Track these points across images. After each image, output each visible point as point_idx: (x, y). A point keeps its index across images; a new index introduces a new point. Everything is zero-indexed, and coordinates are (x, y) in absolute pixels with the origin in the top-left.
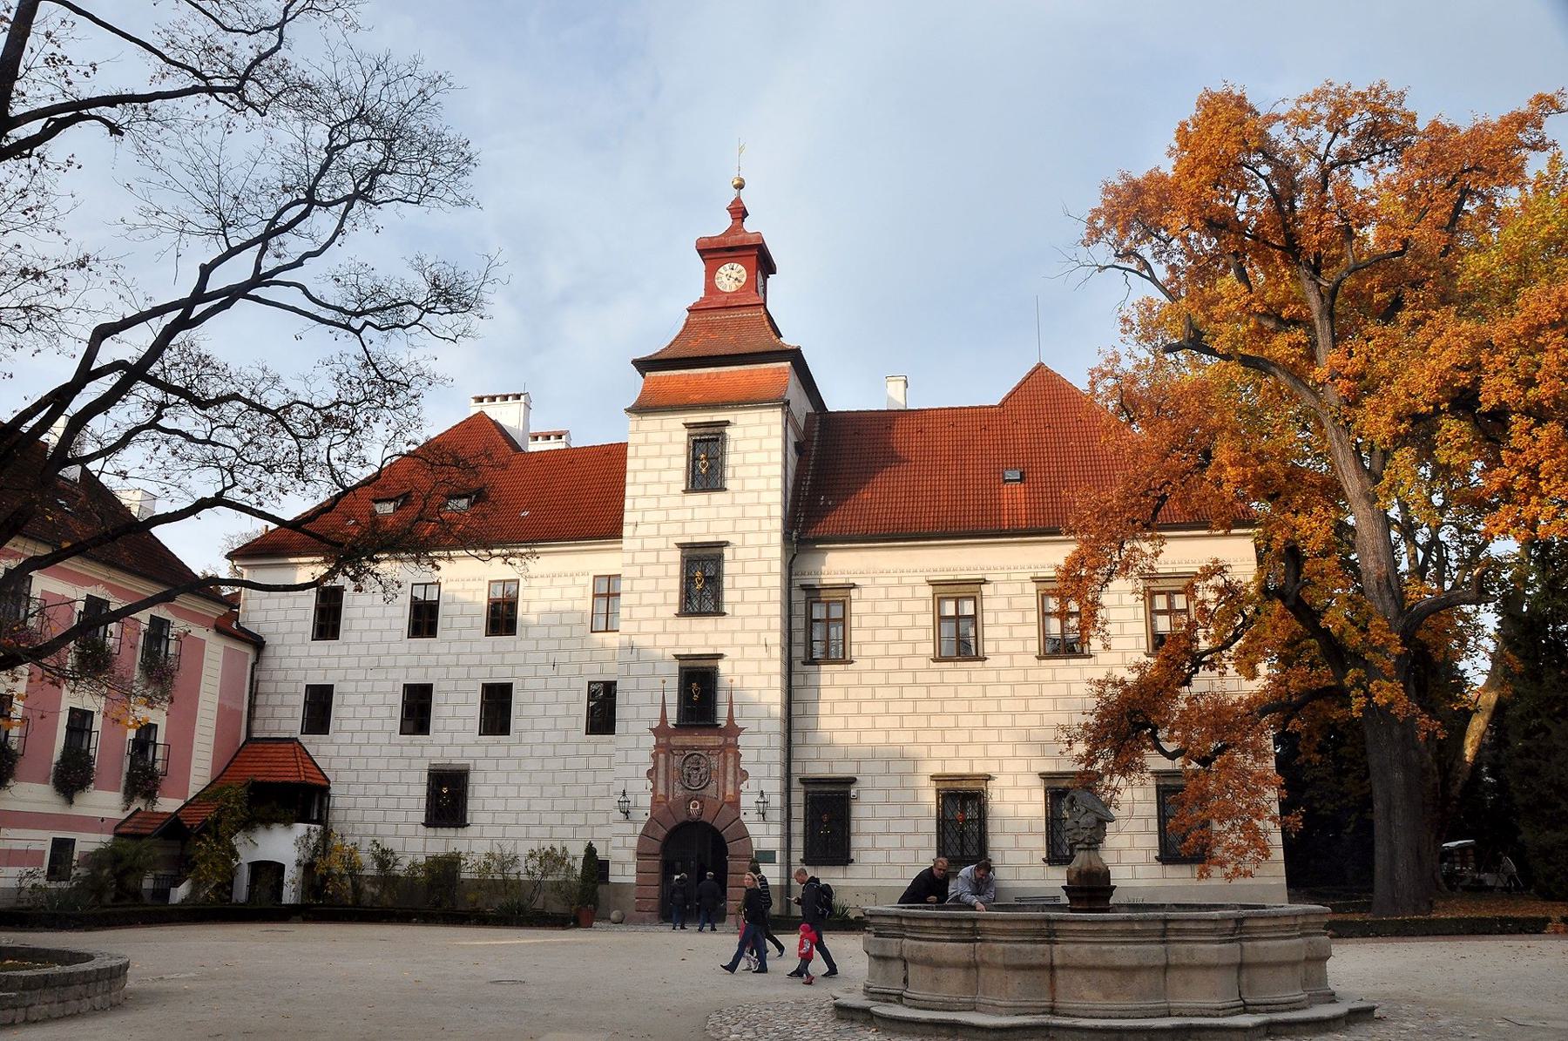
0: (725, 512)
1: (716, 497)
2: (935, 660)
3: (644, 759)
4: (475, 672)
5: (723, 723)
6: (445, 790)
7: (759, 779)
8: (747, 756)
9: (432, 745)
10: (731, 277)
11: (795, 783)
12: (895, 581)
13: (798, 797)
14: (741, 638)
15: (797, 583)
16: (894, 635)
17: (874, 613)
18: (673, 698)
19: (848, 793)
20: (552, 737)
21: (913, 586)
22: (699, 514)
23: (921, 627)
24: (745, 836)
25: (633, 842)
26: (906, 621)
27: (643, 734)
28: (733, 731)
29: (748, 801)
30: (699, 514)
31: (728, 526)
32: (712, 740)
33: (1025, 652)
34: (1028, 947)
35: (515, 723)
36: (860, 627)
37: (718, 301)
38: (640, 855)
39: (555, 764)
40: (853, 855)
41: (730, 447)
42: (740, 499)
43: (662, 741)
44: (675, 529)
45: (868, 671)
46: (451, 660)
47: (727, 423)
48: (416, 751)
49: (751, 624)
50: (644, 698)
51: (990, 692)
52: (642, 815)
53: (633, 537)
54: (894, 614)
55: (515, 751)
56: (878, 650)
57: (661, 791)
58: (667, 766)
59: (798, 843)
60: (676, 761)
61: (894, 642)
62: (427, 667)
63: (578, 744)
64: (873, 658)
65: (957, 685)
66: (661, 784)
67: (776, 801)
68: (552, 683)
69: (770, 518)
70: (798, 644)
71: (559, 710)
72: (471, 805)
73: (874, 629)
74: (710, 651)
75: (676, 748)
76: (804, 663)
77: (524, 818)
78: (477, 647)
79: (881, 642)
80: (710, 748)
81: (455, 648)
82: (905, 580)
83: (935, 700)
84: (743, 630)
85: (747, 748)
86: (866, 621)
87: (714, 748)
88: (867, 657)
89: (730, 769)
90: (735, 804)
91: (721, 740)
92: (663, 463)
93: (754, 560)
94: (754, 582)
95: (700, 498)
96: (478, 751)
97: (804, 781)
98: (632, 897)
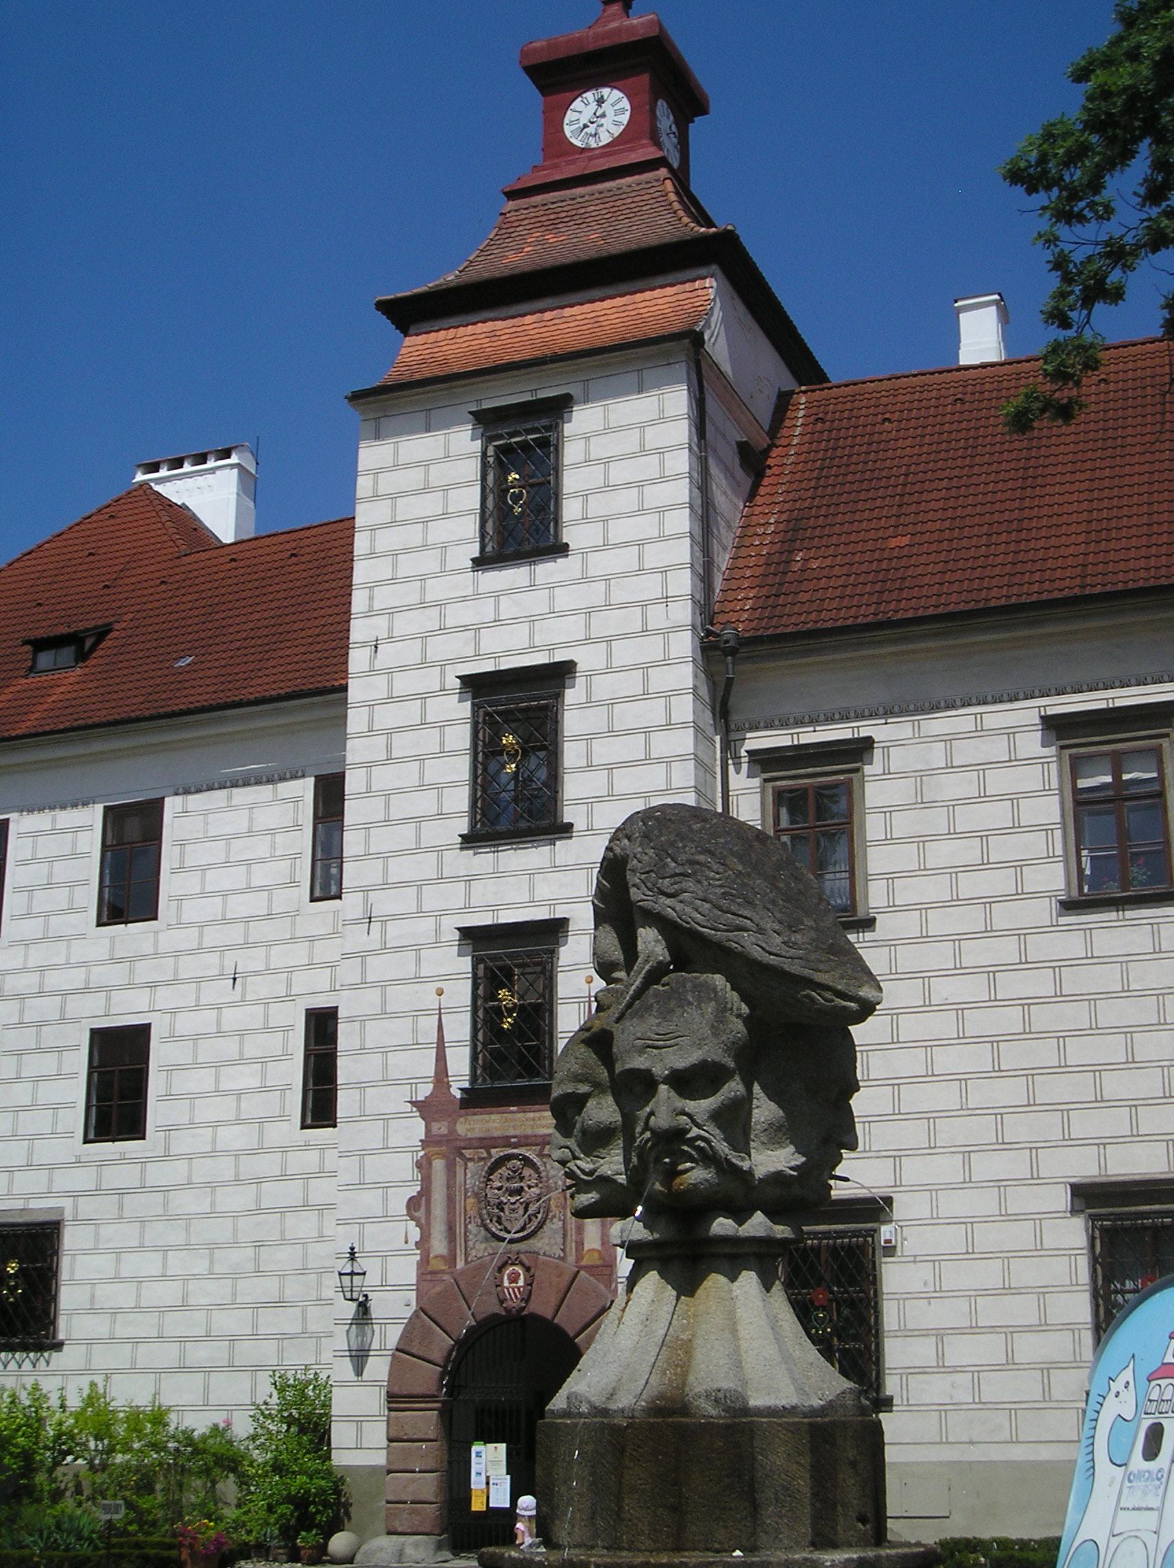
0: (566, 599)
1: (547, 570)
3: (400, 1170)
4: (76, 1006)
16: (969, 852)
17: (923, 803)
18: (460, 1028)
20: (232, 1137)
22: (508, 608)
23: (1033, 829)
26: (998, 814)
27: (398, 1116)
30: (508, 608)
31: (572, 628)
35: (156, 1113)
36: (889, 840)
38: (396, 1400)
39: (240, 1199)
41: (571, 452)
42: (601, 563)
43: (441, 1128)
44: (458, 645)
50: (399, 1030)
52: (395, 1307)
53: (372, 671)
54: (967, 801)
55: (159, 1174)
56: (934, 889)
57: (439, 1246)
58: (450, 1186)
60: (470, 1175)
61: (969, 868)
63: (284, 1150)
64: (923, 908)
65: (1126, 960)
68: (232, 1018)
69: (666, 599)
71: (246, 1078)
72: (69, 1297)
73: (922, 841)
74: (541, 914)
75: (471, 1143)
77: (176, 1324)
78: (80, 951)
79: (938, 871)
81: (37, 956)
83: (1074, 998)
86: (903, 824)
88: (907, 908)
92: (430, 505)
93: (633, 699)
95: (513, 576)
96: (82, 1179)
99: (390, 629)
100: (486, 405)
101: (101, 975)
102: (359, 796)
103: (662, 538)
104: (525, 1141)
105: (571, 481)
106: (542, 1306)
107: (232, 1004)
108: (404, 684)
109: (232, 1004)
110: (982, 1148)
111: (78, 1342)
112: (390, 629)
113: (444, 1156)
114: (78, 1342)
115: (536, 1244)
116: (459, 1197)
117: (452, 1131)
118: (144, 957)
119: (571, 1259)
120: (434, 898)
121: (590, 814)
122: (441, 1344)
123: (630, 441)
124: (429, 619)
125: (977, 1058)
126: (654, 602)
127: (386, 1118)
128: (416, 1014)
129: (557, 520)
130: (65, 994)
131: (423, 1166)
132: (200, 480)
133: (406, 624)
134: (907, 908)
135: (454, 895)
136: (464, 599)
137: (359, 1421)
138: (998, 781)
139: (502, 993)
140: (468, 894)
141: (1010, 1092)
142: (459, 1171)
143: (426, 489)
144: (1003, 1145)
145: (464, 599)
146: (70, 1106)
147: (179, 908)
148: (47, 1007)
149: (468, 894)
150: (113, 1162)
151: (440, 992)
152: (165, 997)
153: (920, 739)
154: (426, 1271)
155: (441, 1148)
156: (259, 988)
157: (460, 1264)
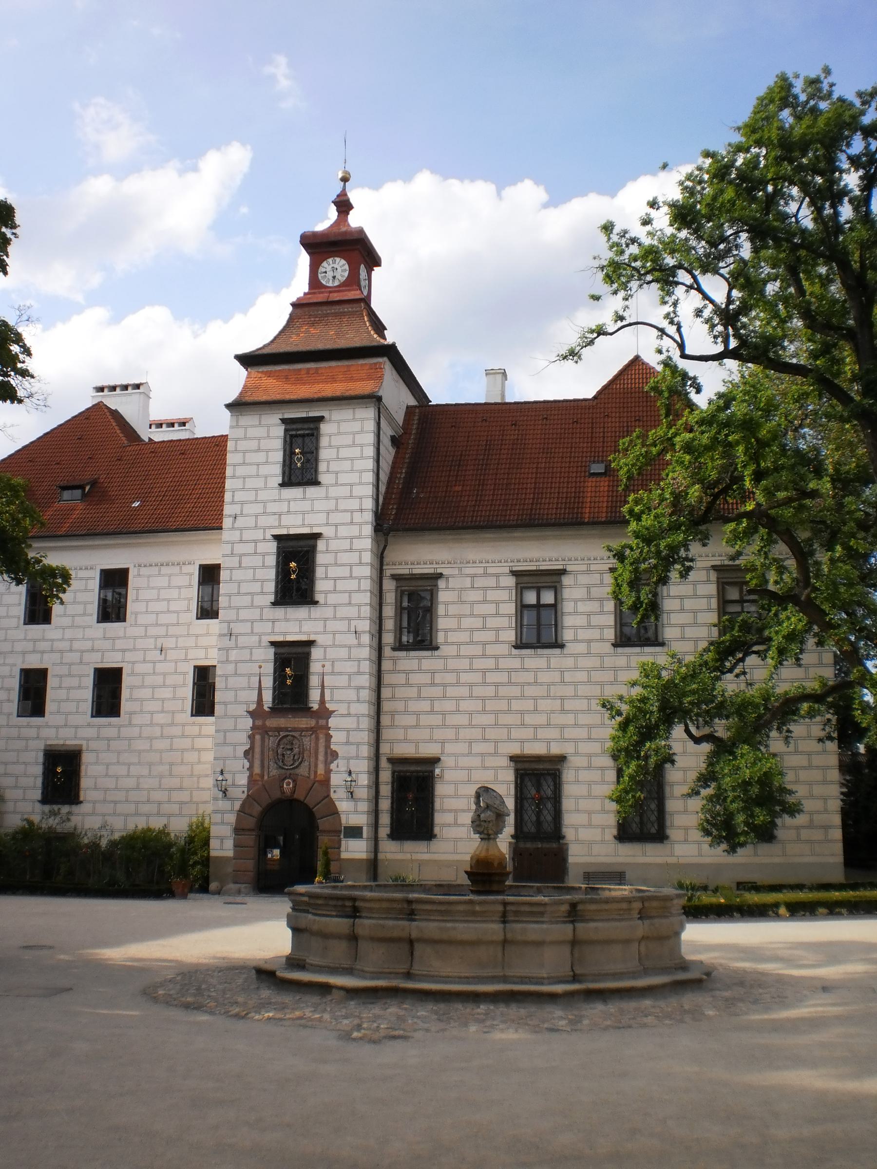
0: (319, 505)
1: (312, 491)
2: (516, 647)
3: (241, 739)
4: (87, 657)
5: (315, 706)
6: (59, 770)
7: (348, 759)
8: (337, 737)
9: (48, 726)
10: (336, 269)
11: (384, 763)
12: (481, 571)
13: (386, 776)
14: (332, 626)
15: (388, 573)
16: (478, 623)
18: (268, 682)
19: (432, 772)
21: (497, 576)
22: (294, 506)
23: (503, 616)
24: (335, 813)
25: (232, 818)
26: (490, 609)
28: (324, 713)
29: (336, 779)
30: (294, 506)
32: (304, 722)
33: (602, 640)
34: (391, 923)
35: (125, 706)
36: (446, 616)
37: (320, 298)
40: (437, 830)
41: (324, 441)
42: (334, 492)
43: (259, 723)
44: (272, 521)
45: (453, 657)
46: (65, 645)
47: (321, 419)
48: (33, 732)
49: (342, 612)
50: (242, 682)
51: (568, 677)
52: (240, 793)
53: (233, 528)
54: (479, 602)
56: (463, 637)
57: (257, 770)
59: (385, 819)
60: (271, 742)
61: (478, 630)
62: (43, 652)
63: (184, 725)
64: (459, 644)
65: (536, 671)
66: (257, 763)
67: (364, 780)
69: (361, 510)
70: (389, 631)
72: (85, 783)
73: (460, 617)
74: (304, 638)
76: (394, 649)
78: (89, 633)
79: (466, 630)
80: (302, 730)
81: (69, 634)
82: (490, 571)
84: (335, 618)
85: (338, 729)
86: (452, 610)
87: (307, 730)
88: (453, 644)
89: (322, 750)
90: (326, 782)
91: (313, 723)
92: (260, 457)
93: (346, 551)
94: (345, 571)
96: (91, 732)
97: (392, 761)
98: (230, 870)
99: (242, 511)
100: (286, 416)
101: (99, 644)
102: (226, 582)
103: (360, 483)
104: (295, 730)
105: (324, 454)
106: (299, 795)
107: (160, 661)
108: (248, 535)
109: (160, 661)
110: (476, 741)
111: (89, 802)
112: (242, 511)
113: (260, 734)
114: (89, 802)
115: (297, 771)
116: (266, 750)
117: (264, 724)
118: (119, 638)
119: (312, 777)
120: (259, 627)
121: (326, 598)
122: (257, 809)
123: (348, 440)
124: (258, 508)
125: (477, 705)
126: (357, 511)
127: (236, 717)
128: (250, 675)
129: (316, 471)
130: (82, 652)
131: (251, 737)
132: (124, 399)
133: (249, 509)
134: (453, 644)
135: (268, 627)
136: (275, 501)
137: (222, 839)
138: (492, 595)
139: (288, 670)
140: (273, 627)
141: (488, 719)
142: (267, 740)
143: (259, 450)
144: (485, 740)
145: (275, 501)
146: (85, 701)
147: (136, 618)
148: (74, 657)
149: (273, 627)
150: (104, 726)
151: (260, 667)
152: (129, 656)
153: (461, 575)
154: (251, 780)
155: (259, 730)
156: (172, 655)
157: (266, 777)
